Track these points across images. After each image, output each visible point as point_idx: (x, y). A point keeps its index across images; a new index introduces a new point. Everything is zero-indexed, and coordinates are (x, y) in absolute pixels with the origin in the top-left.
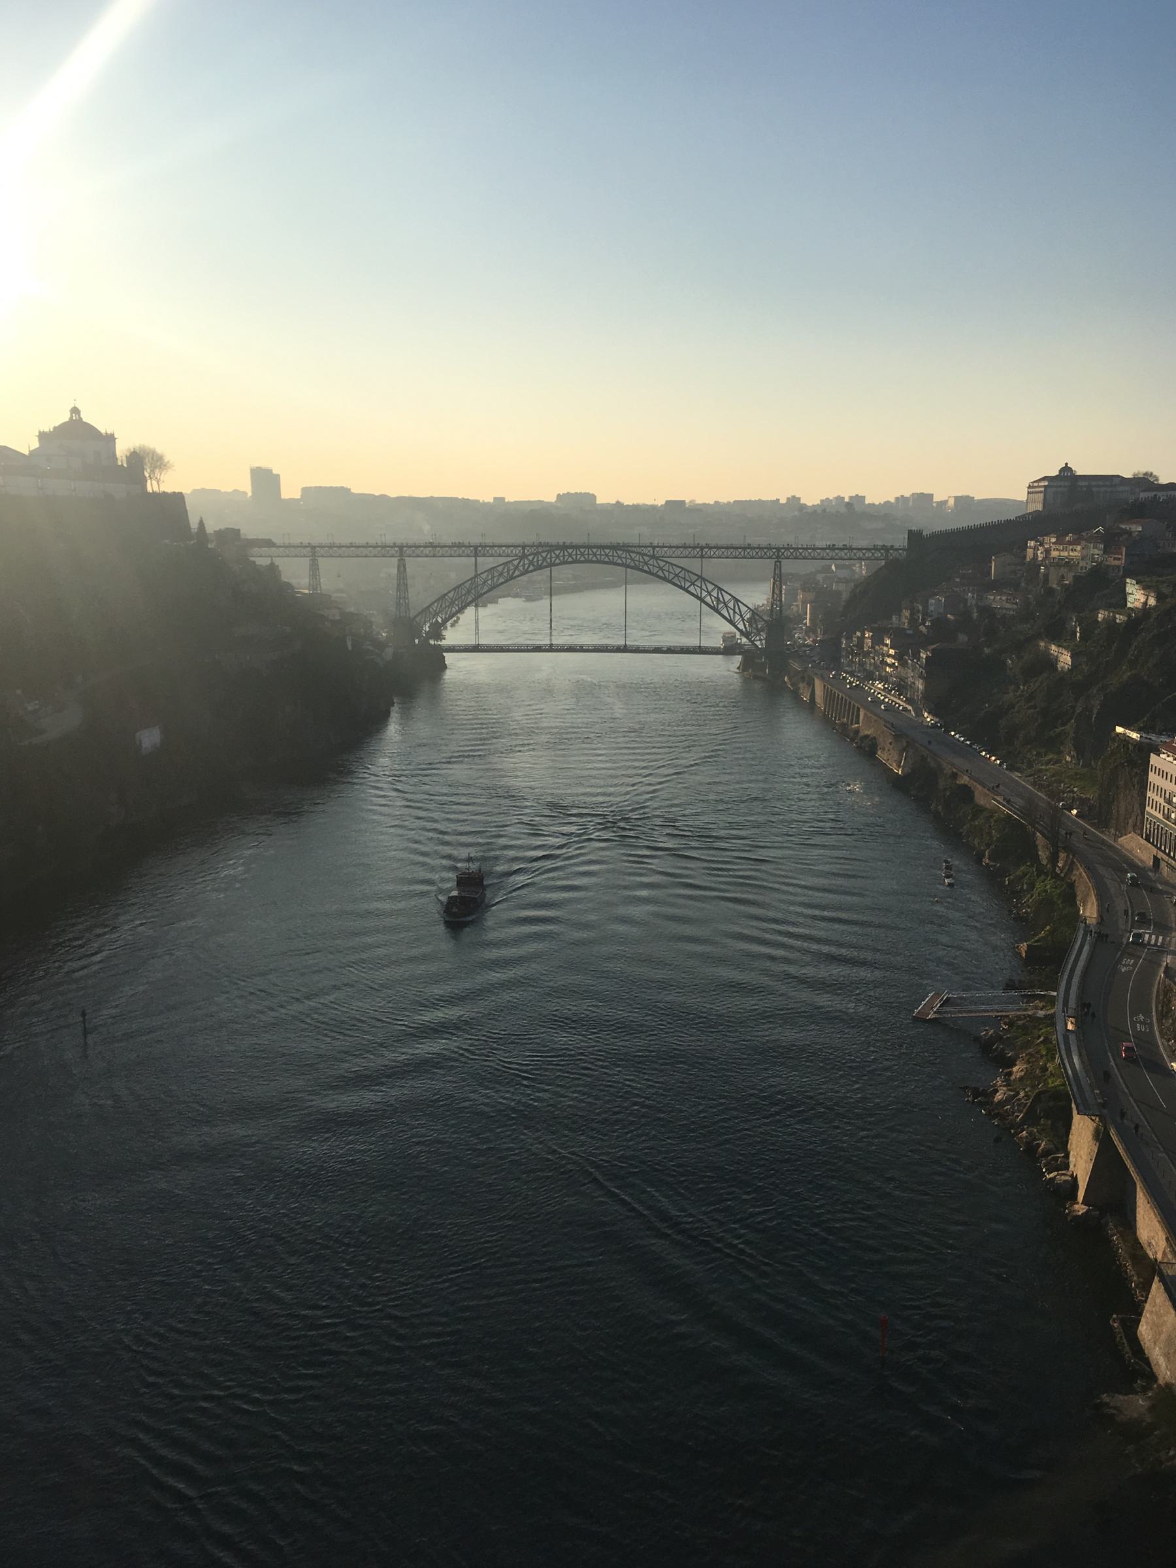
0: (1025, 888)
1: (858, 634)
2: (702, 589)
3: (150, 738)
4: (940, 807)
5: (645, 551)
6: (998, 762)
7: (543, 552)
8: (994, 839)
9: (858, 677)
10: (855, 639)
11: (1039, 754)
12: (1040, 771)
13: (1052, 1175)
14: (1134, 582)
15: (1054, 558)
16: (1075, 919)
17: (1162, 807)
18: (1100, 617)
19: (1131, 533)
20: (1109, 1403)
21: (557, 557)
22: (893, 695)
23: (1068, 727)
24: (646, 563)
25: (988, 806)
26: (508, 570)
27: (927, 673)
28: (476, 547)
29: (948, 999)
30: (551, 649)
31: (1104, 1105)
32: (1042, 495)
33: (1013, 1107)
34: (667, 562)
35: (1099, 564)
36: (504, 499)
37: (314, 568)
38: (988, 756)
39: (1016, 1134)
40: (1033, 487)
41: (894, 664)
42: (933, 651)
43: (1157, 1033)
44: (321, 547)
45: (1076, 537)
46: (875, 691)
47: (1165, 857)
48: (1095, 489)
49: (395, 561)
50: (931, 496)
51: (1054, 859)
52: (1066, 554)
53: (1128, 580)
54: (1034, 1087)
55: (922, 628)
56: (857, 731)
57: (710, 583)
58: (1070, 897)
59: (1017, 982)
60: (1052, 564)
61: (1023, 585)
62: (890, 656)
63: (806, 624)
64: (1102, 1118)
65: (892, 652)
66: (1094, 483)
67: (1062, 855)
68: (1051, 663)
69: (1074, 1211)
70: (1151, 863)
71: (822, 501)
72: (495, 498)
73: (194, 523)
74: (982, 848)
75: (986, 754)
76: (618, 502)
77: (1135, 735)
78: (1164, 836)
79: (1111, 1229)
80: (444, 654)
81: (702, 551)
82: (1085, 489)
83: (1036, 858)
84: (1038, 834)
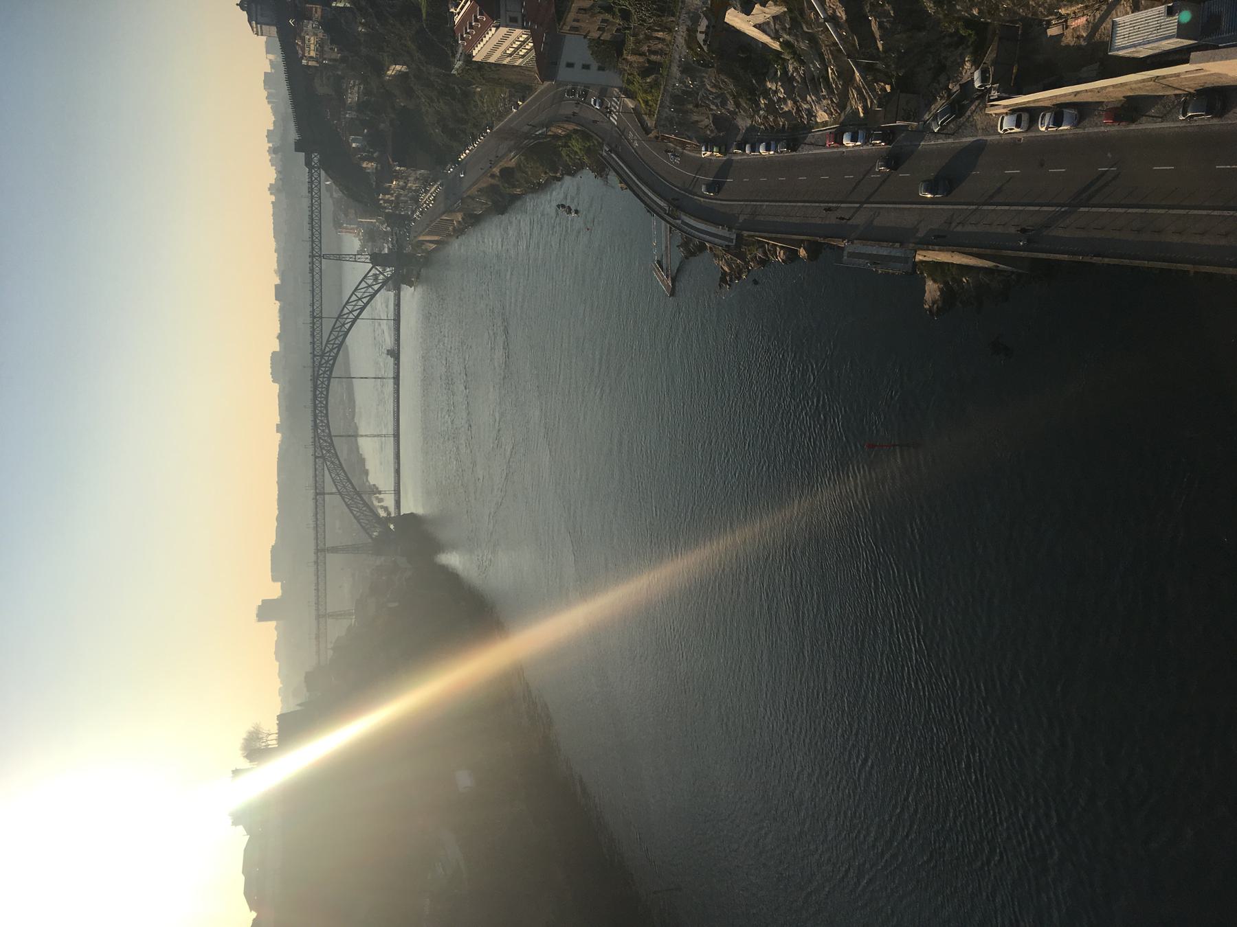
1: (381, 202)
2: (347, 318)
11: (476, 106)
15: (316, 54)
21: (323, 431)
24: (327, 362)
28: (317, 494)
29: (659, 262)
30: (397, 436)
32: (263, 26)
34: (326, 345)
35: (320, 24)
40: (257, 31)
44: (317, 610)
45: (298, 38)
49: (330, 556)
52: (312, 47)
55: (375, 155)
56: (459, 222)
68: (401, 75)
71: (272, 165)
80: (402, 514)
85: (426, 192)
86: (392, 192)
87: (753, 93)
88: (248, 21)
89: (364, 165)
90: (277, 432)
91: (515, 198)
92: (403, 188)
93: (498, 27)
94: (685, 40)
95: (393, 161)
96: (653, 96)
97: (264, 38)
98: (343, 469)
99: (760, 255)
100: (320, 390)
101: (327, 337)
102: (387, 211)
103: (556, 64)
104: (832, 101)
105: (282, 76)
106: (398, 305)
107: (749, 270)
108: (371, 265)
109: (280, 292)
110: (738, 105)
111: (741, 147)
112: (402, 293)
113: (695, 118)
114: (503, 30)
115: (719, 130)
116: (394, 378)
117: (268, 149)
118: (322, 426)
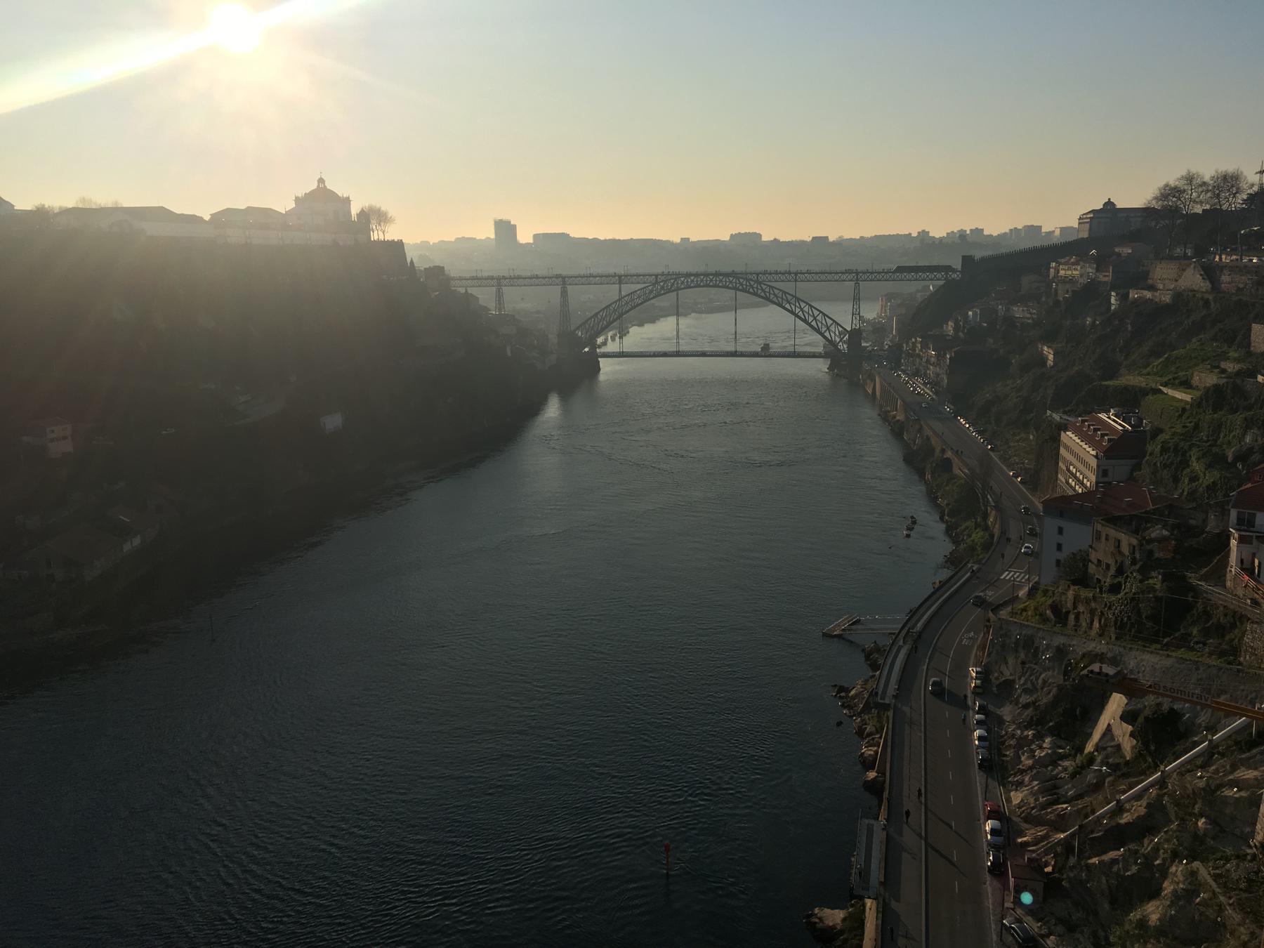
1: (913, 340)
3: (333, 422)
4: (929, 476)
7: (672, 279)
9: (907, 374)
10: (911, 344)
15: (1061, 276)
19: (1120, 254)
28: (620, 277)
29: (858, 622)
30: (678, 354)
32: (1087, 226)
34: (769, 286)
35: (1093, 280)
36: (689, 239)
37: (499, 295)
40: (1082, 219)
44: (504, 278)
49: (558, 289)
50: (1040, 227)
52: (1069, 272)
55: (961, 334)
56: (894, 417)
61: (1044, 299)
68: (1043, 360)
71: (947, 233)
73: (409, 260)
80: (599, 359)
81: (795, 276)
85: (925, 384)
86: (924, 350)
87: (1038, 722)
88: (1092, 211)
89: (950, 323)
90: (682, 239)
91: (921, 473)
92: (928, 361)
93: (1096, 457)
94: (1091, 651)
95: (955, 352)
96: (1032, 616)
97: (1076, 226)
98: (645, 302)
99: (869, 729)
100: (724, 280)
102: (905, 345)
104: (1033, 808)
105: (1037, 244)
106: (814, 356)
107: (852, 717)
108: (849, 329)
109: (820, 241)
110: (1026, 706)
111: (982, 710)
112: (821, 360)
113: (1011, 661)
114: (1093, 463)
116: (736, 351)
118: (688, 282)
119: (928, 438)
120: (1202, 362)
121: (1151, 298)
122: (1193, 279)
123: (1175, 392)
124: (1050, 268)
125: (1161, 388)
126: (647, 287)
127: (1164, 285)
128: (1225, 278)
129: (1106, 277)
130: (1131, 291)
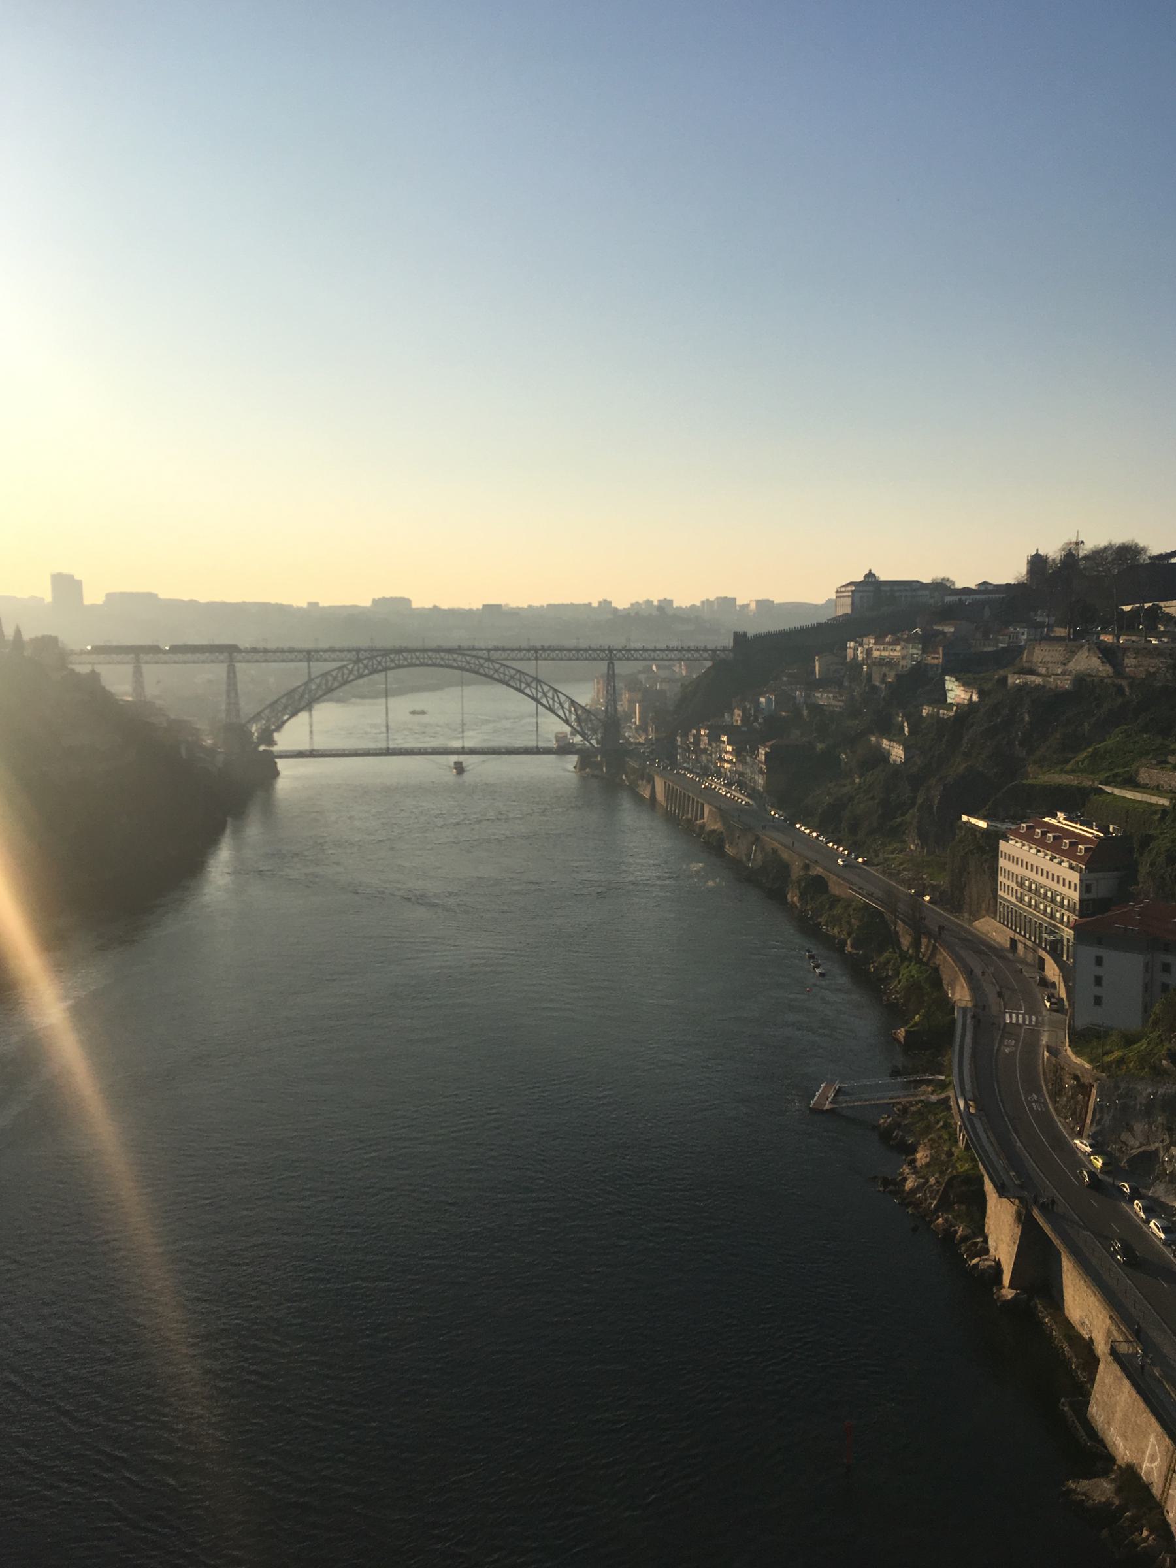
0: (890, 974)
1: (694, 732)
4: (795, 899)
5: (480, 654)
6: (846, 852)
8: (855, 927)
9: (696, 773)
12: (886, 860)
13: (975, 1261)
14: (953, 679)
15: (875, 658)
16: (947, 1006)
17: (1014, 891)
18: (924, 712)
20: (1076, 1490)
22: (735, 790)
23: (908, 817)
24: (482, 666)
25: (844, 896)
26: (343, 674)
27: (767, 768)
28: (309, 652)
29: (840, 1088)
30: (388, 752)
31: (1022, 1187)
32: (849, 600)
33: (925, 1194)
34: (502, 665)
35: (919, 663)
38: (836, 847)
39: (932, 1222)
41: (732, 759)
42: (771, 747)
43: (1053, 1113)
46: (716, 787)
47: (1022, 938)
48: (897, 594)
50: (735, 599)
51: (916, 944)
53: (947, 678)
54: (942, 1173)
56: (702, 826)
57: (544, 683)
58: (936, 982)
59: (901, 1068)
60: (874, 663)
61: (846, 684)
62: (726, 752)
63: (635, 723)
64: (1021, 1200)
65: (729, 748)
66: (896, 588)
67: (924, 941)
68: (884, 757)
69: (1003, 1296)
70: (1008, 945)
71: (632, 605)
72: (374, 600)
74: (843, 936)
75: (833, 845)
76: (435, 607)
77: (983, 824)
78: (1018, 919)
79: (1042, 1312)
81: (537, 652)
82: (888, 594)
83: (898, 944)
84: (899, 922)
85: (729, 785)
86: (714, 745)
89: (737, 712)
91: (776, 895)
93: (1071, 867)
95: (772, 745)
97: (834, 598)
101: (514, 666)
102: (679, 739)
103: (1099, 942)
112: (552, 757)
113: (1139, 1127)
114: (1075, 877)
115: (1132, 1160)
116: (537, 747)
117: (651, 599)
119: (775, 851)
120: (1141, 757)
121: (1041, 683)
122: (1087, 662)
123: (1124, 791)
124: (847, 647)
125: (1100, 786)
126: (344, 666)
127: (1047, 668)
128: (1130, 661)
129: (936, 659)
130: (1009, 676)
